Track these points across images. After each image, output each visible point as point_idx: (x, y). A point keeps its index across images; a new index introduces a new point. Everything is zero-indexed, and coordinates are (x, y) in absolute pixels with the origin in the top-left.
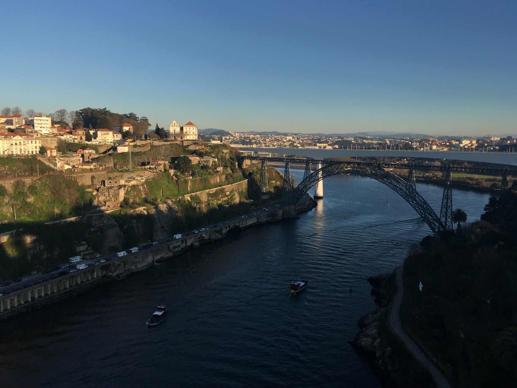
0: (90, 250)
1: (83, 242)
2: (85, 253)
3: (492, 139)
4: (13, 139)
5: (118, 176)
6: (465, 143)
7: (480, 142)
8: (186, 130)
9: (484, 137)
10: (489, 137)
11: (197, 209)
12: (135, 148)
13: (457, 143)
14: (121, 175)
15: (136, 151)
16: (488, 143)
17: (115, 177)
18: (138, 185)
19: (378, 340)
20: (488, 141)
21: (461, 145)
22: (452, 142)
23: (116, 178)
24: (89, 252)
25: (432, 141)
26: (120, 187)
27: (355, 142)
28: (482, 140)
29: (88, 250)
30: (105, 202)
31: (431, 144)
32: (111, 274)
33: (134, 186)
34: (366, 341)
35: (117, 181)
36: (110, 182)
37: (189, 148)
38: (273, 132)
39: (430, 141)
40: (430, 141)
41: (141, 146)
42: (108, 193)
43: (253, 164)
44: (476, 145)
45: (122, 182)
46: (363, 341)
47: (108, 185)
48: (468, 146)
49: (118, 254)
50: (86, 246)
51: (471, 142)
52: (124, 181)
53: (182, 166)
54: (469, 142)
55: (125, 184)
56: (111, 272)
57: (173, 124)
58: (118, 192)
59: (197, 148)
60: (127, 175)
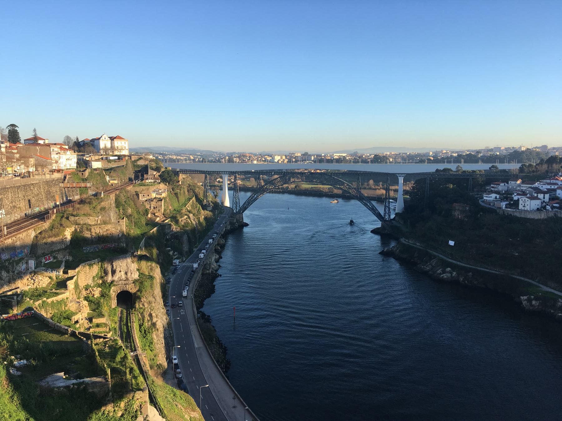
0: (176, 255)
1: (168, 248)
2: (175, 257)
3: (296, 155)
4: (67, 154)
5: (144, 189)
6: (277, 158)
7: (288, 157)
8: (121, 145)
9: (289, 153)
10: (293, 153)
11: (201, 219)
12: (109, 163)
13: (271, 158)
14: (147, 188)
15: (111, 166)
16: (295, 158)
17: (142, 191)
18: (166, 198)
19: (455, 273)
20: (294, 157)
21: (276, 161)
22: (266, 158)
23: (143, 192)
24: (177, 256)
25: (249, 156)
26: (160, 200)
27: (162, 158)
28: (288, 156)
29: (175, 255)
30: (154, 214)
31: (249, 159)
32: (208, 272)
33: (163, 198)
34: (446, 275)
35: (149, 194)
36: (144, 195)
37: (138, 163)
38: (373, 147)
39: (247, 156)
40: (247, 156)
41: (116, 161)
42: (150, 206)
43: (184, 178)
44: (287, 160)
45: (154, 195)
46: (444, 276)
47: (141, 198)
48: (282, 162)
49: (200, 256)
50: (172, 251)
51: (281, 158)
52: (155, 194)
53: (168, 179)
54: (279, 157)
55: (157, 197)
56: (208, 270)
57: (104, 139)
58: (160, 204)
59: (146, 163)
60: (152, 189)
